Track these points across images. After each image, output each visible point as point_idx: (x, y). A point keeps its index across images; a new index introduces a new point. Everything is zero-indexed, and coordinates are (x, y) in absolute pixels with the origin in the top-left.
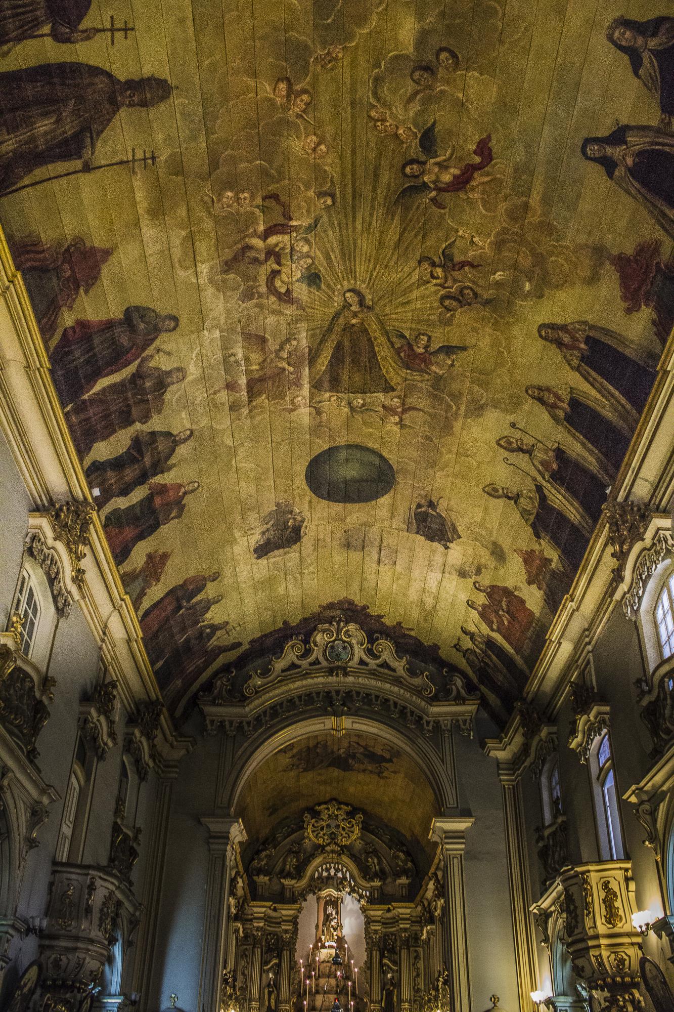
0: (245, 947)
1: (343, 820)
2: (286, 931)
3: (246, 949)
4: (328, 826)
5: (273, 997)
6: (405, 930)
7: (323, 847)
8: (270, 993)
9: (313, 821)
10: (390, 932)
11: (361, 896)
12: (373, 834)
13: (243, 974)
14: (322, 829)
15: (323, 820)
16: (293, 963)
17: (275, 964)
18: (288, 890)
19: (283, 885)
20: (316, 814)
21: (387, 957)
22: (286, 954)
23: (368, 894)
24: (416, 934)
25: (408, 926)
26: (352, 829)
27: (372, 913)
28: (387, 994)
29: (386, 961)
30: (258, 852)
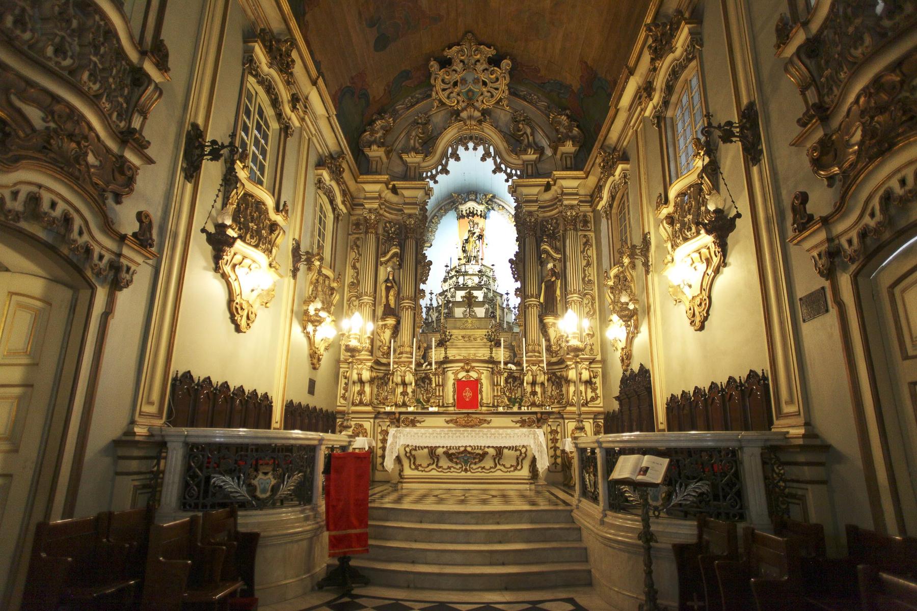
0: (357, 236)
1: (483, 71)
2: (410, 216)
3: (358, 239)
4: (464, 81)
5: (392, 293)
6: (572, 207)
7: (456, 114)
8: (388, 289)
9: (441, 72)
10: (549, 217)
11: (510, 176)
12: (524, 99)
13: (354, 267)
14: (455, 84)
15: (455, 71)
16: (420, 256)
17: (395, 255)
18: (413, 169)
19: (405, 163)
20: (445, 63)
21: (547, 242)
22: (411, 244)
23: (519, 173)
24: (585, 216)
25: (576, 202)
26: (496, 85)
27: (525, 191)
28: (546, 287)
29: (545, 247)
30: (372, 123)
